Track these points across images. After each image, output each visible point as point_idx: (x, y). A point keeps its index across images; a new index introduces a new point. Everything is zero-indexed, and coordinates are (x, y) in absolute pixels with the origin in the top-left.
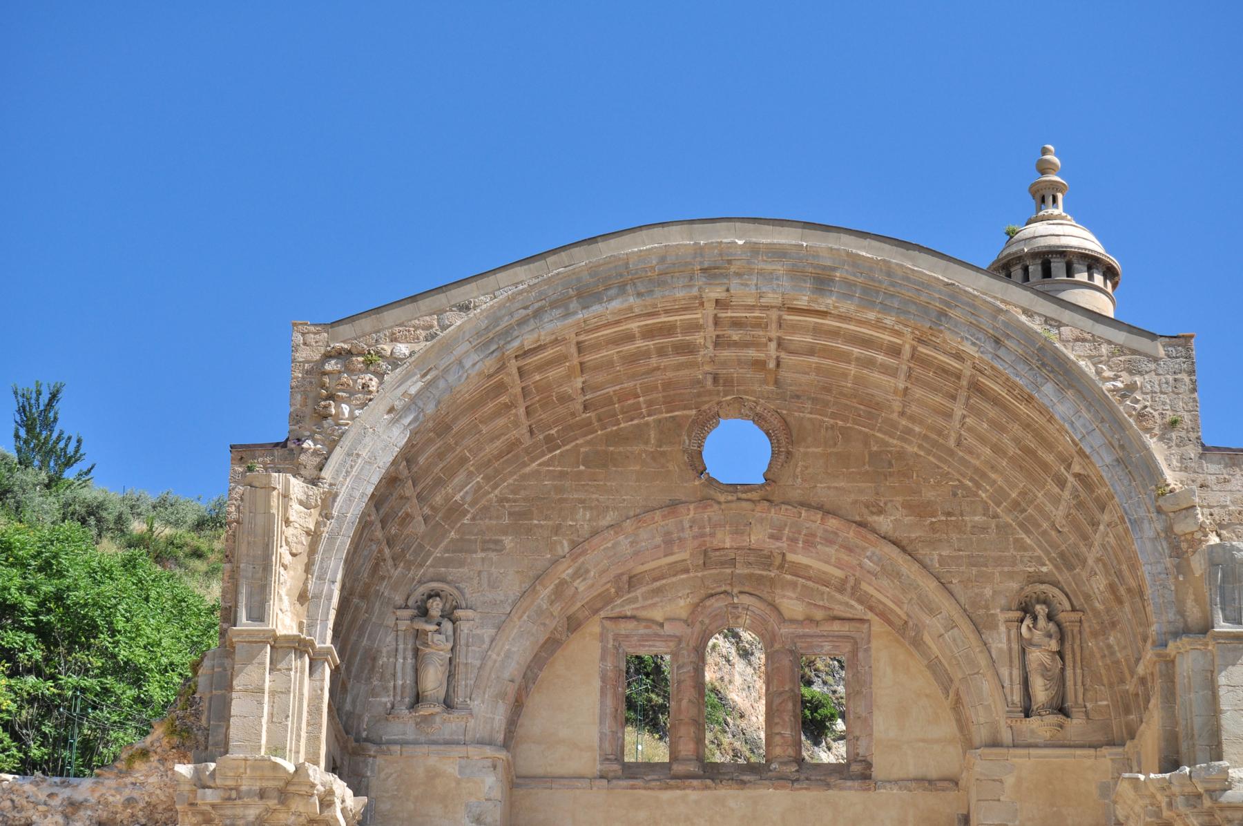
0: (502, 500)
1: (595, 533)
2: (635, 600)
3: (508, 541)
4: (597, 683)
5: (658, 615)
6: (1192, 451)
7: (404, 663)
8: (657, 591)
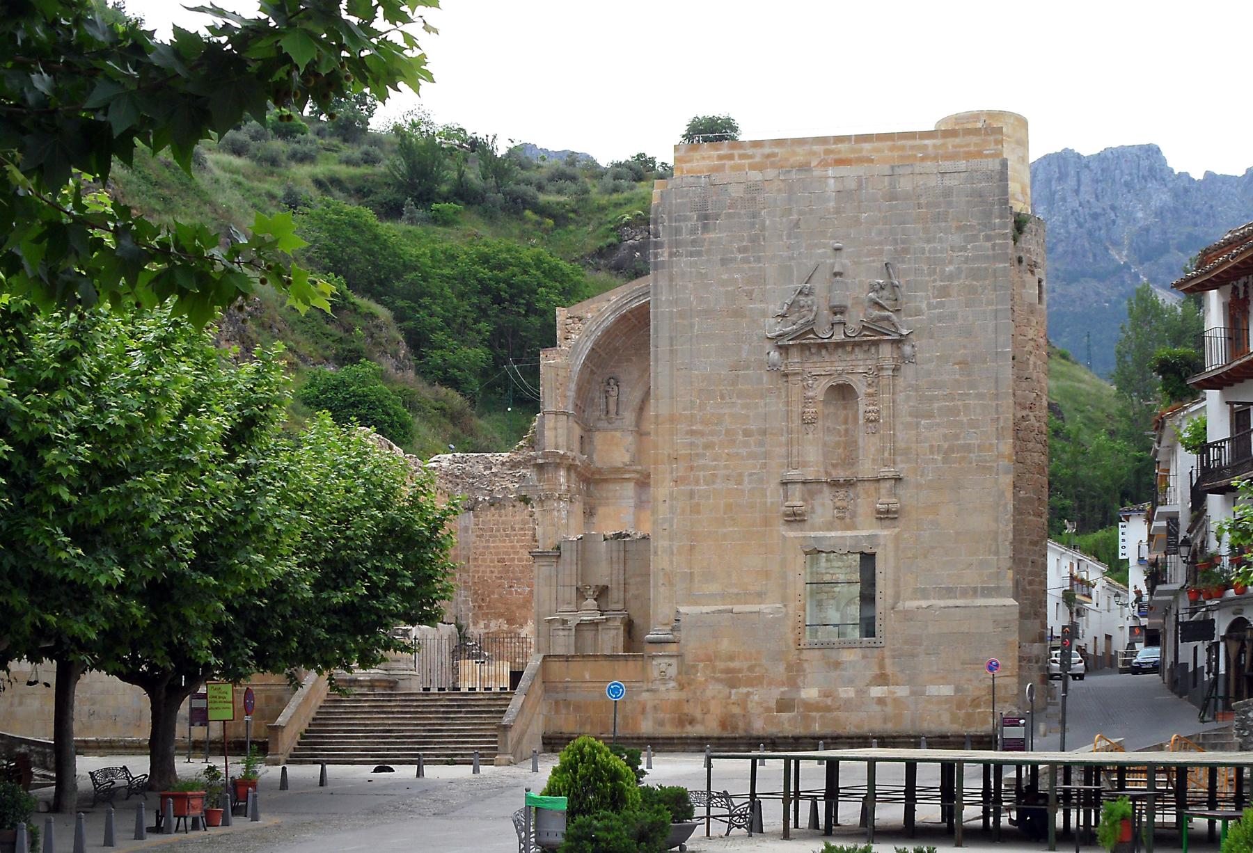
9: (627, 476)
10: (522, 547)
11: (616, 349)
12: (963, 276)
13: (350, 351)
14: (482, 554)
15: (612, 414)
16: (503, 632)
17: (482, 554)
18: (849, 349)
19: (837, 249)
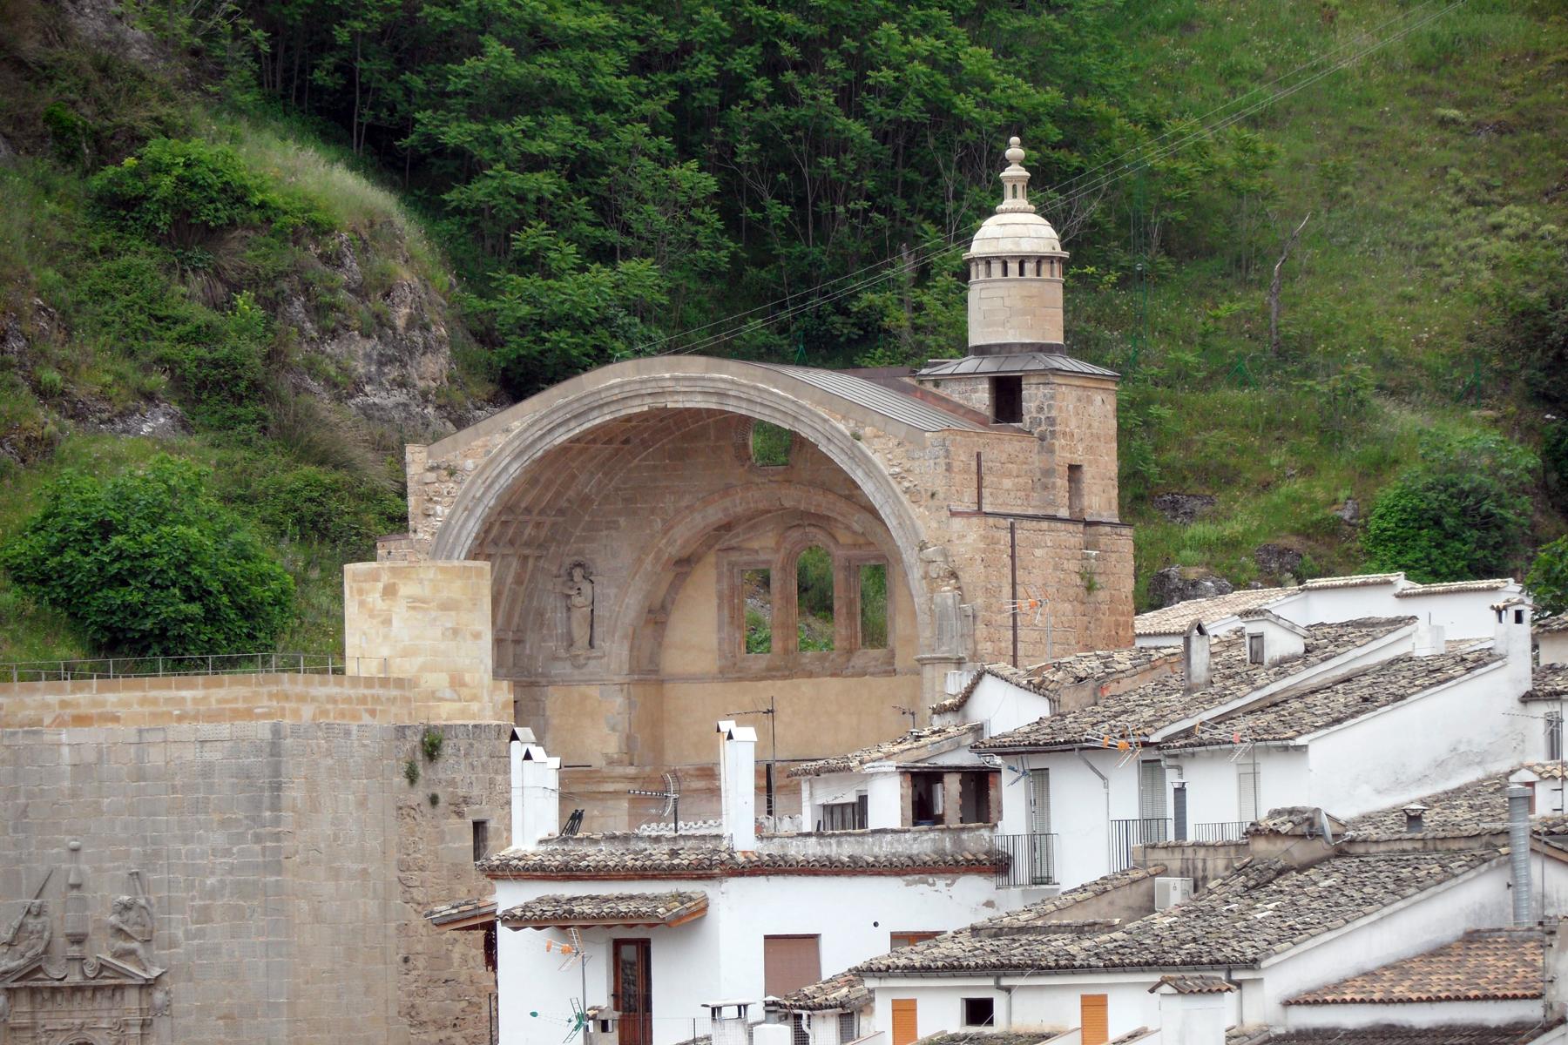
0: (617, 489)
1: (677, 512)
2: (737, 535)
3: (622, 521)
4: (715, 602)
5: (756, 545)
7: (560, 615)
8: (753, 527)
9: (610, 787)
11: (585, 501)
12: (227, 892)
13: (216, 364)
18: (89, 994)
19: (75, 850)
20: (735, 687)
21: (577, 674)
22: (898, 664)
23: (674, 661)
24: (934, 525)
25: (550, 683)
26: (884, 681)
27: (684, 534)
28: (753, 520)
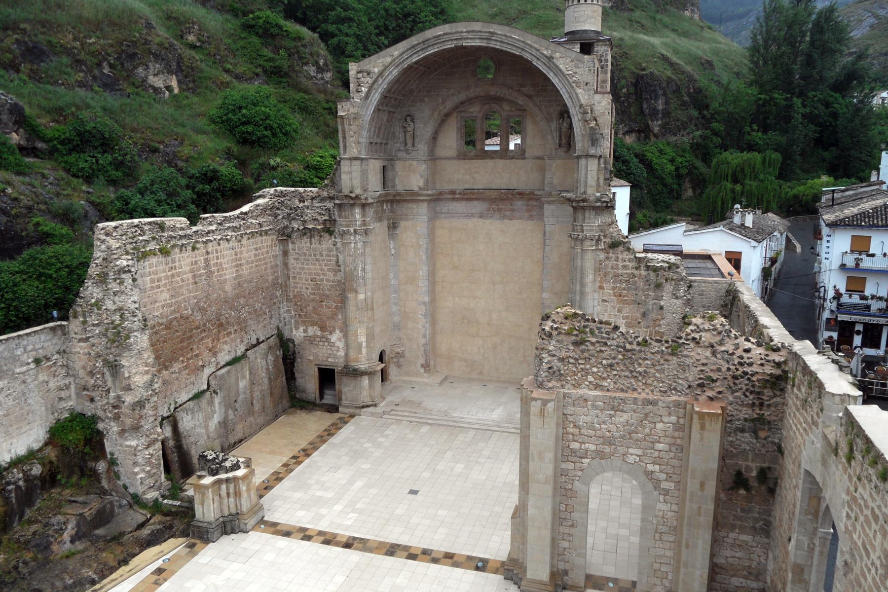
3: (426, 99)
5: (471, 110)
6: (592, 92)
7: (402, 135)
9: (421, 198)
10: (329, 270)
11: (412, 91)
13: (275, 67)
14: (299, 274)
15: (410, 144)
16: (317, 336)
17: (299, 274)
20: (462, 162)
21: (408, 156)
22: (527, 155)
23: (440, 152)
24: (586, 97)
25: (398, 159)
26: (521, 162)
27: (449, 105)
28: (470, 101)
